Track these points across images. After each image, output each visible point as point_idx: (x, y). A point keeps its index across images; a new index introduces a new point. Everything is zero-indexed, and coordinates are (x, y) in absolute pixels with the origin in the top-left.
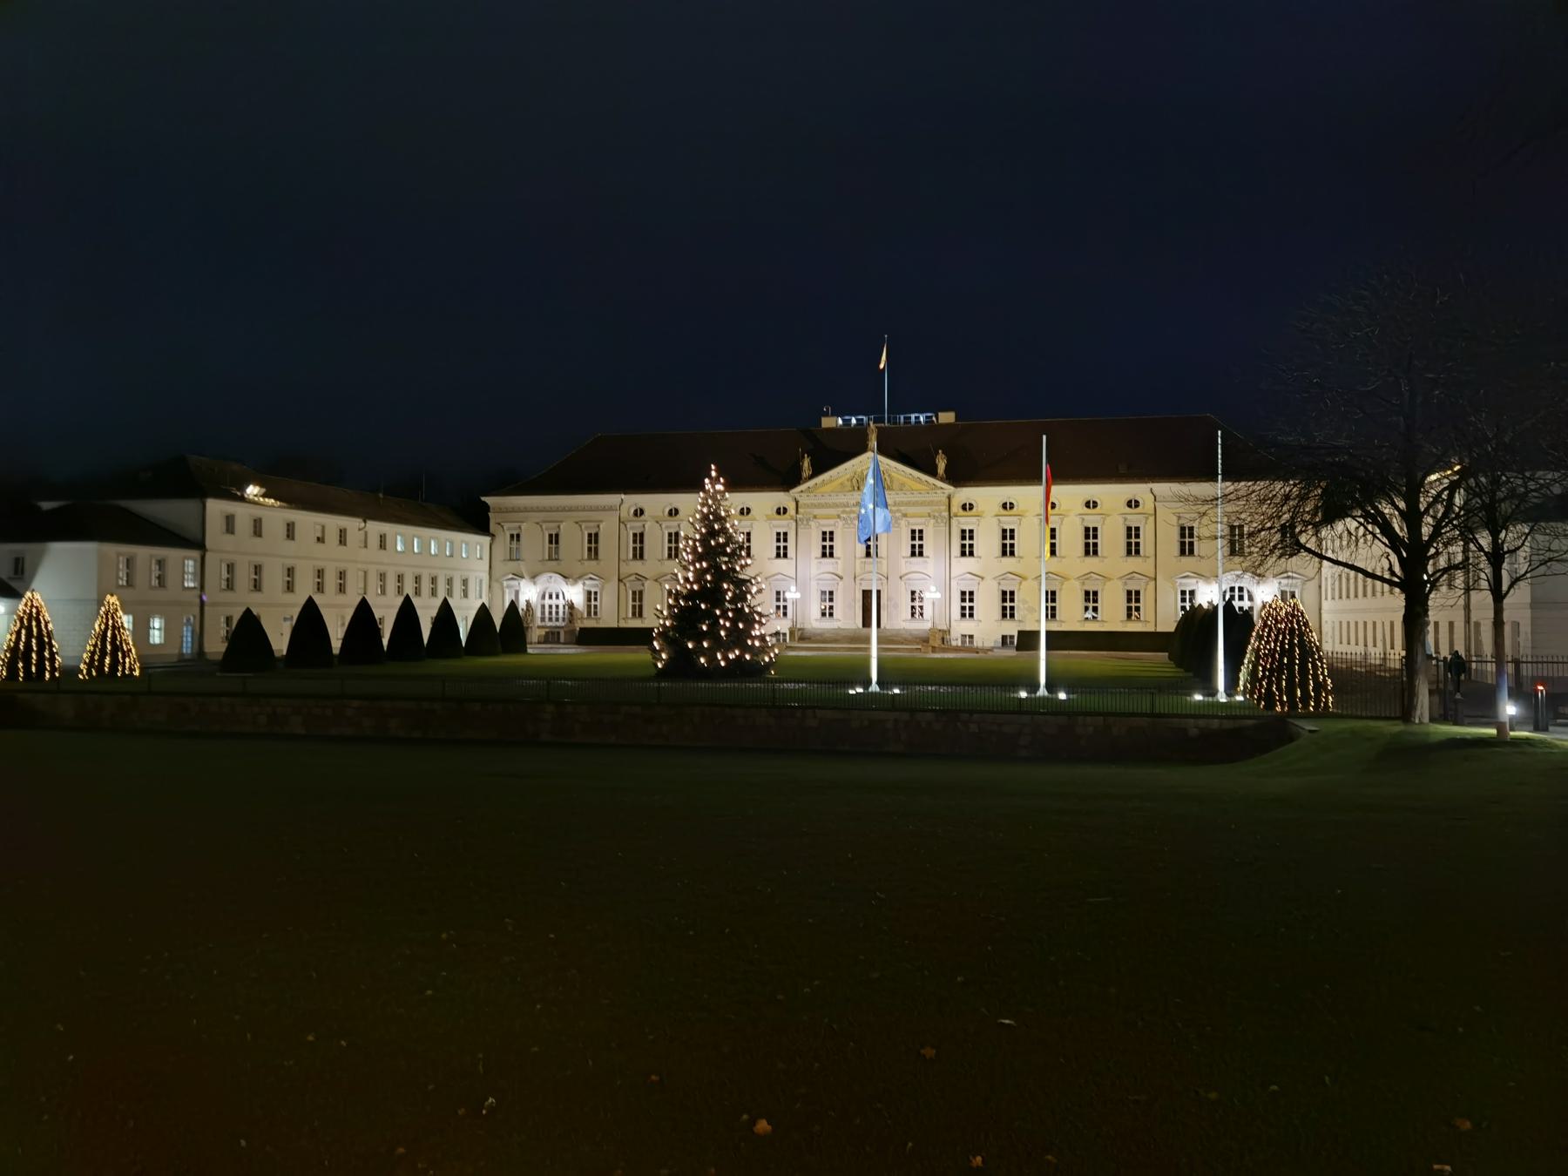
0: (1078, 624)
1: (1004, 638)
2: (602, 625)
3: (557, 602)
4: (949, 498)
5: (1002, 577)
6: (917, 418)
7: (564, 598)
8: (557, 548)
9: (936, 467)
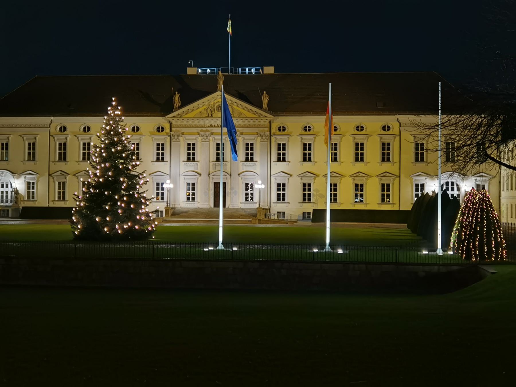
0: (351, 205)
1: (304, 213)
2: (37, 205)
3: (7, 189)
4: (270, 123)
5: (303, 175)
6: (250, 70)
7: (12, 187)
8: (7, 153)
9: (262, 102)
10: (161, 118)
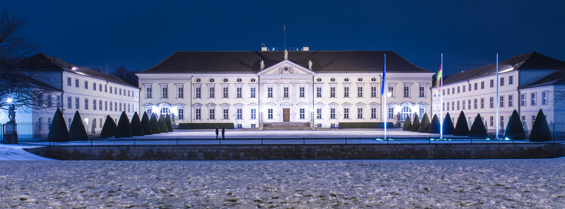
4: (313, 77)
7: (169, 112)
10: (254, 74)
